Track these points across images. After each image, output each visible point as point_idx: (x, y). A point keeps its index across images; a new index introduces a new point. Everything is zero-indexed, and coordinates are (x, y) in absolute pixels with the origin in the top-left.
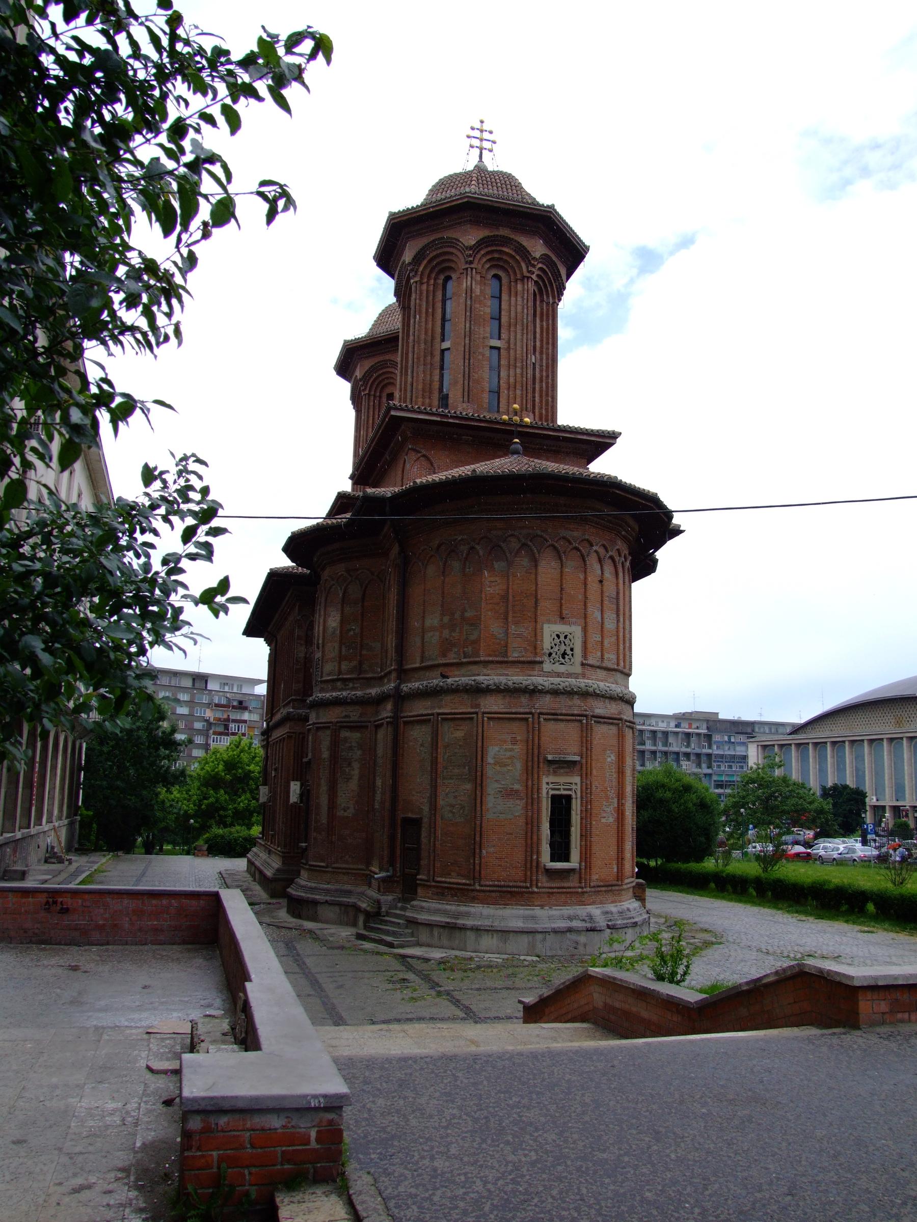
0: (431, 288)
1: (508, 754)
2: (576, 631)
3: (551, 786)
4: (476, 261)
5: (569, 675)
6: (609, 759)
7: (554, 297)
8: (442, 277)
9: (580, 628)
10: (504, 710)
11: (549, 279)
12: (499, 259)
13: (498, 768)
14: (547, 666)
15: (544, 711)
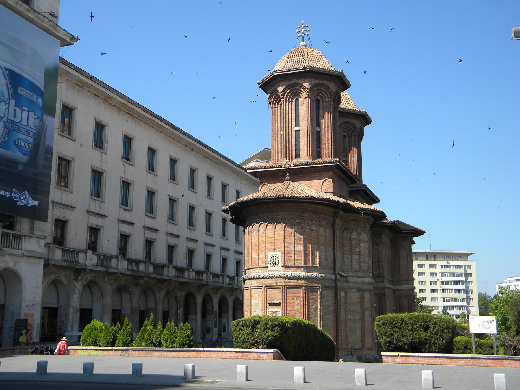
0: (276, 109)
1: (257, 301)
2: (280, 255)
3: (269, 313)
4: (285, 97)
5: (277, 271)
6: (296, 302)
7: (329, 99)
8: (280, 104)
9: (281, 252)
10: (256, 286)
11: (324, 91)
12: (296, 92)
13: (255, 307)
14: (269, 268)
15: (266, 285)
